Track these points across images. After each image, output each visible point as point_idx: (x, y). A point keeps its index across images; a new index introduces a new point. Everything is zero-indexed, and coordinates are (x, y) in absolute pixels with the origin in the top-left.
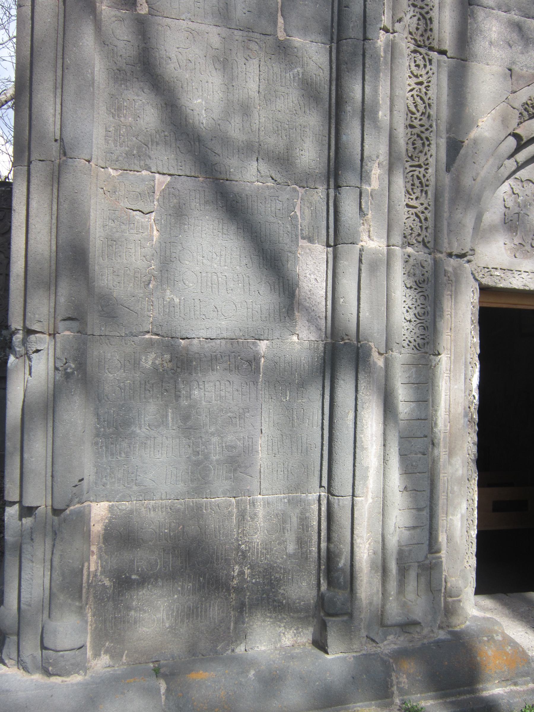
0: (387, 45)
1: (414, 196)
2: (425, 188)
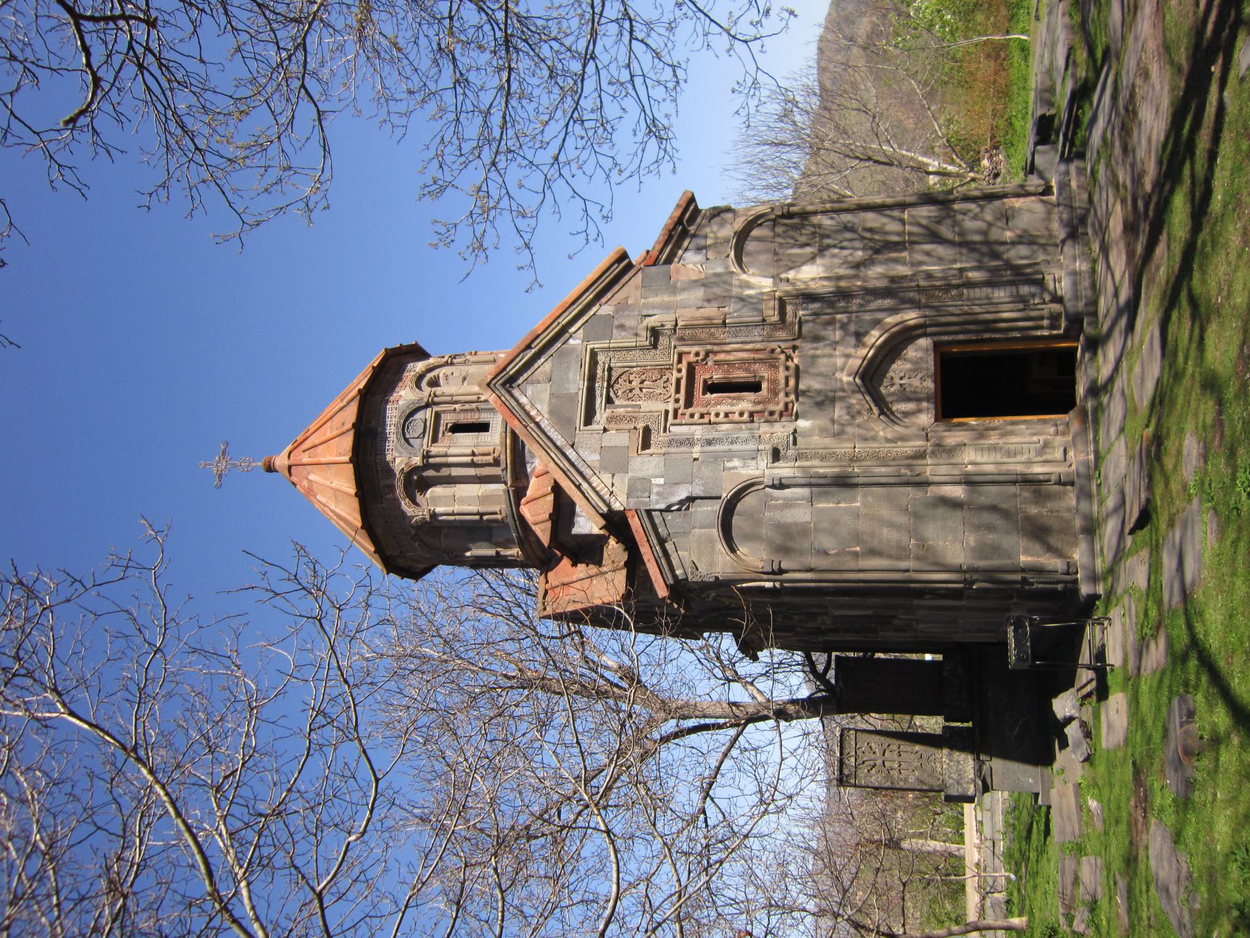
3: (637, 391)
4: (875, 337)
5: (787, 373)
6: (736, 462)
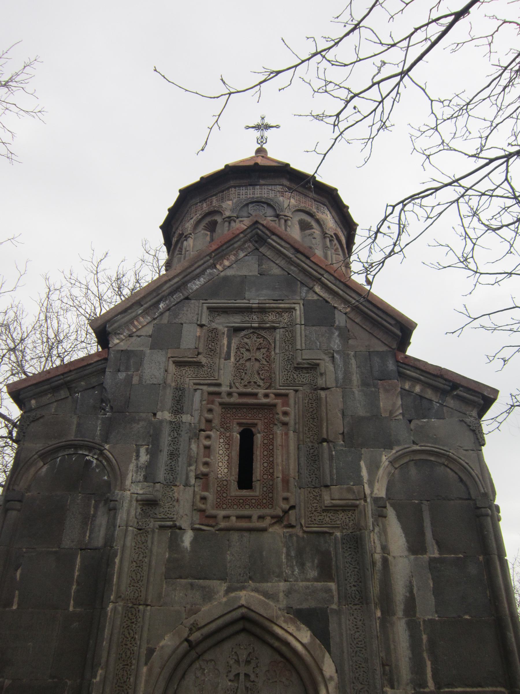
0: (112, 609)
1: (122, 681)
2: (129, 676)
3: (247, 355)
4: (300, 637)
5: (255, 518)
6: (144, 458)
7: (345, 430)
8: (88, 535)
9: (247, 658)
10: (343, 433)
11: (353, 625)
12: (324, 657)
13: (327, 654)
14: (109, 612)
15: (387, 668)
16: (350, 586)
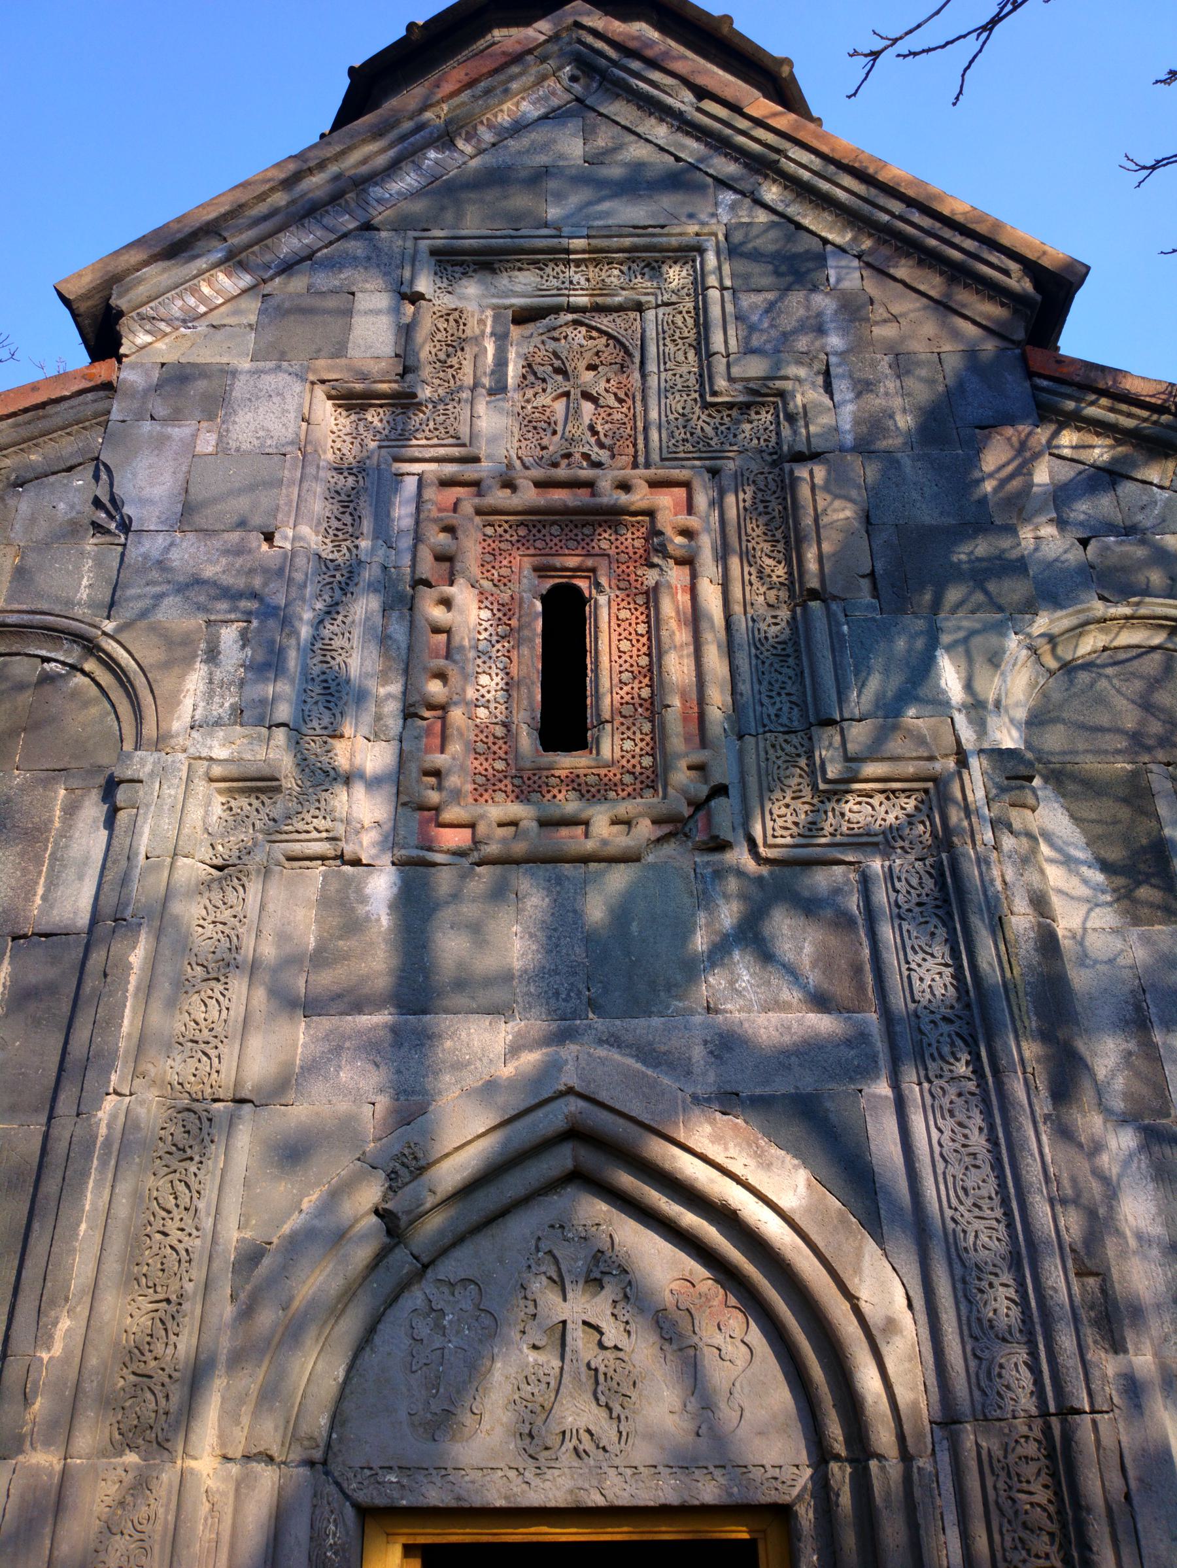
7: (879, 567)
8: (40, 891)
9: (590, 1271)
10: (872, 574)
11: (957, 1146)
12: (859, 1255)
13: (871, 1246)
14: (103, 1125)
15: (1091, 1281)
16: (933, 1022)
